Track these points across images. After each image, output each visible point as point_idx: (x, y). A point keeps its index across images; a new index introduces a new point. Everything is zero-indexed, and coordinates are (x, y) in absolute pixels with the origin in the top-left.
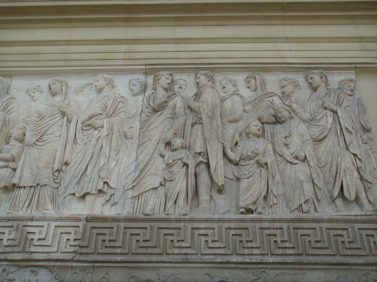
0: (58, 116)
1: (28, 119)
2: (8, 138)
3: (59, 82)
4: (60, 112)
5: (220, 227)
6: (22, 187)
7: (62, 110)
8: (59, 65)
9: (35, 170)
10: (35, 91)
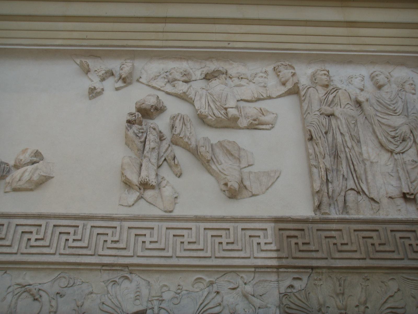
5: (235, 229)
8: (355, 49)
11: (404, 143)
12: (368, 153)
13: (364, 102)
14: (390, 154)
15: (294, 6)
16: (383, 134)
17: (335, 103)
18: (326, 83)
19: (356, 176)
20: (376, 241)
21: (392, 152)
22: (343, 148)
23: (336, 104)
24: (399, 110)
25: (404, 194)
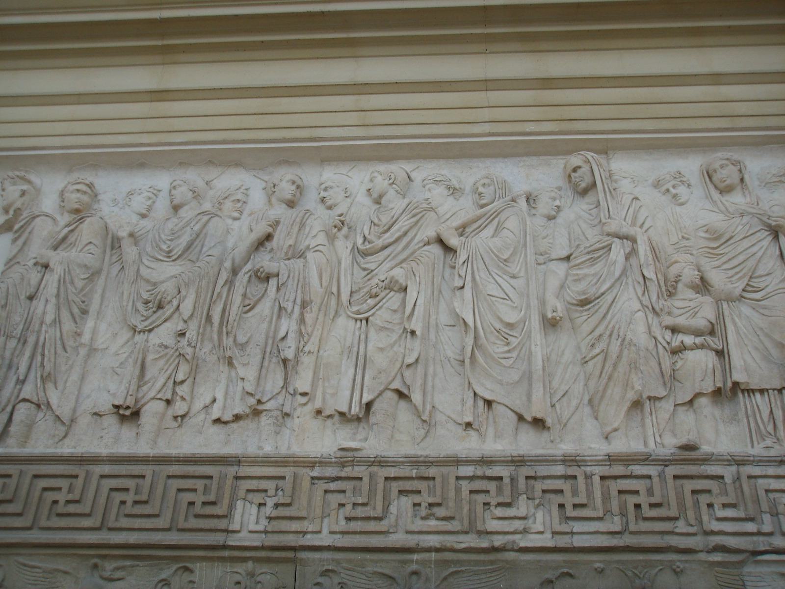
0: (764, 235)
1: (685, 243)
2: (672, 285)
3: (733, 164)
4: (765, 228)
6: (753, 391)
7: (774, 224)
9: (775, 353)
10: (676, 182)
11: (160, 312)
12: (94, 332)
13: (123, 238)
14: (130, 334)
15: (419, 55)
16: (134, 297)
17: (70, 242)
18: (76, 206)
19: (42, 376)
20: (642, 499)
21: (134, 330)
22: (37, 326)
23: (71, 244)
24: (177, 251)
25: (117, 407)
